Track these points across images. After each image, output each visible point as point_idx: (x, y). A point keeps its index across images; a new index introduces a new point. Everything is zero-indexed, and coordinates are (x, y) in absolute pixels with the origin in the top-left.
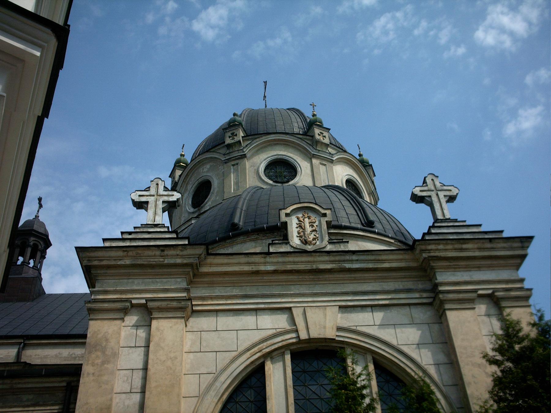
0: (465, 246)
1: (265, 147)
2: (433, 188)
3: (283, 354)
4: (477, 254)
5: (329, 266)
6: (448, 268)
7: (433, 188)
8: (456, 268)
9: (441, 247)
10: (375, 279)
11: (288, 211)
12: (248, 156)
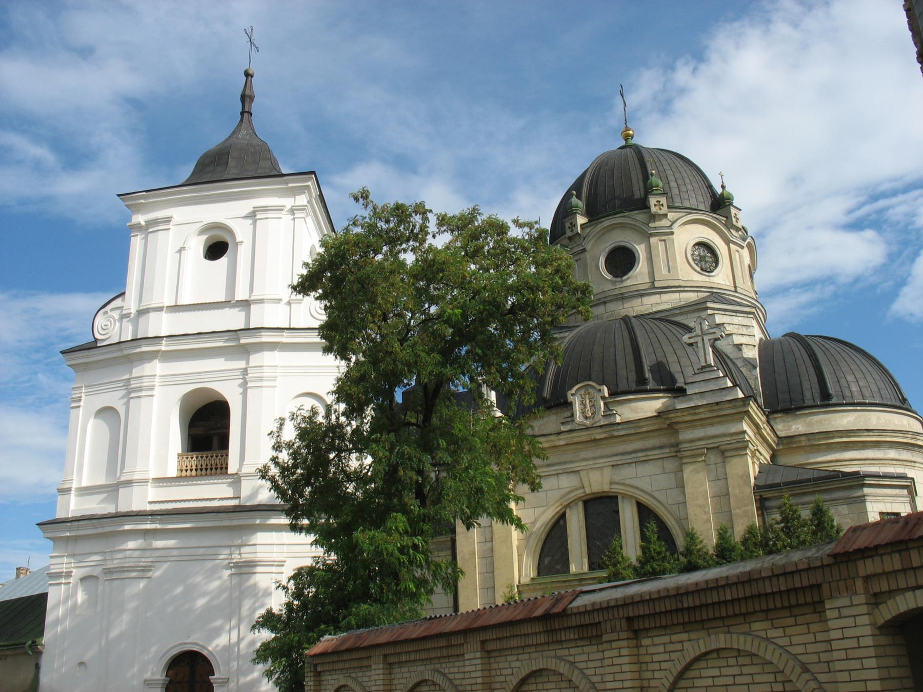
0: (697, 411)
1: (603, 234)
4: (708, 415)
5: (602, 436)
6: (687, 428)
8: (694, 427)
9: (679, 414)
12: (588, 247)
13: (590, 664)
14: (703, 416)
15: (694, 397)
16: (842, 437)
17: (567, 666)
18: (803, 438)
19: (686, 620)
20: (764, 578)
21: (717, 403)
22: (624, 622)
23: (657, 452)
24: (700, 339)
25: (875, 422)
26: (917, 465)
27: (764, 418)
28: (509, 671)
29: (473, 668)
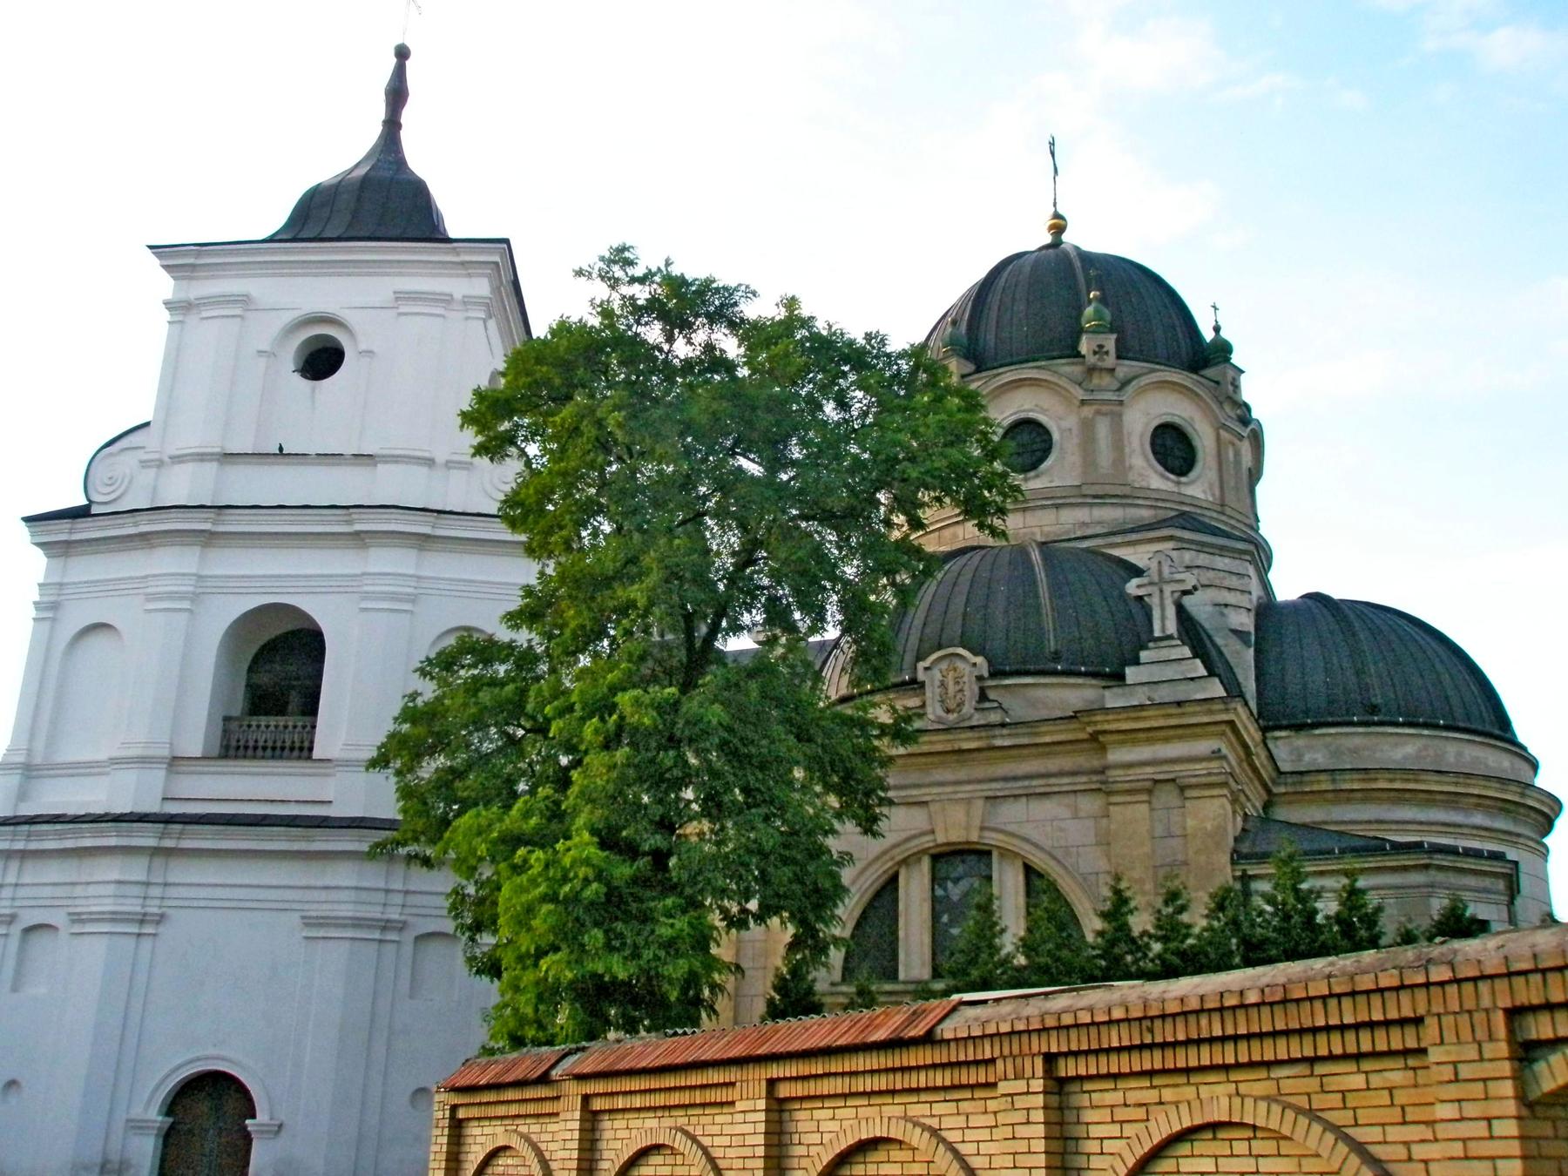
0: (1144, 714)
2: (1156, 579)
3: (919, 860)
6: (1123, 743)
7: (1156, 579)
8: (1135, 742)
9: (1110, 717)
10: (1037, 756)
11: (927, 663)
13: (970, 1135)
14: (1155, 724)
15: (1140, 689)
16: (1391, 781)
17: (926, 1135)
18: (1322, 777)
19: (1158, 1065)
20: (1311, 999)
21: (1179, 704)
22: (1039, 1062)
23: (1066, 780)
24: (1154, 590)
25: (1452, 760)
26: (1521, 840)
27: (1258, 736)
28: (816, 1138)
29: (749, 1128)
